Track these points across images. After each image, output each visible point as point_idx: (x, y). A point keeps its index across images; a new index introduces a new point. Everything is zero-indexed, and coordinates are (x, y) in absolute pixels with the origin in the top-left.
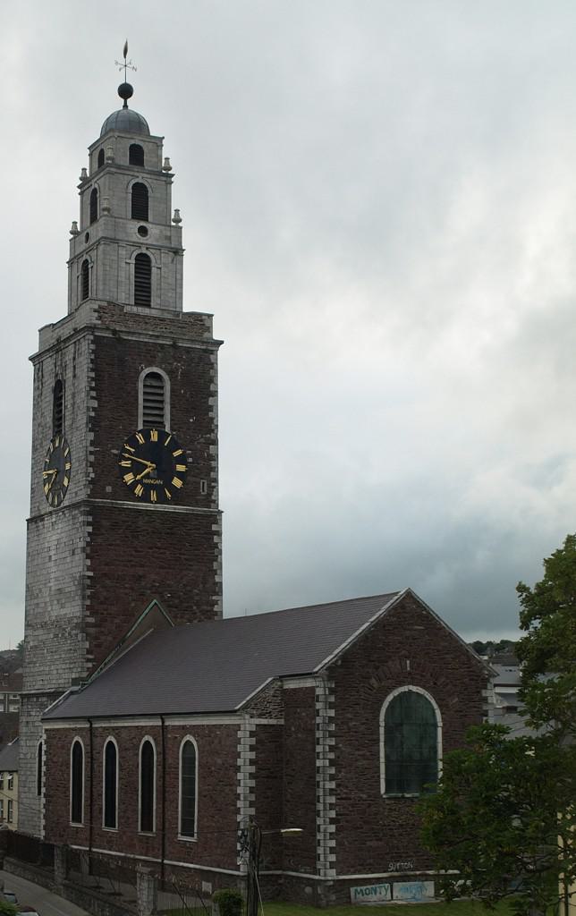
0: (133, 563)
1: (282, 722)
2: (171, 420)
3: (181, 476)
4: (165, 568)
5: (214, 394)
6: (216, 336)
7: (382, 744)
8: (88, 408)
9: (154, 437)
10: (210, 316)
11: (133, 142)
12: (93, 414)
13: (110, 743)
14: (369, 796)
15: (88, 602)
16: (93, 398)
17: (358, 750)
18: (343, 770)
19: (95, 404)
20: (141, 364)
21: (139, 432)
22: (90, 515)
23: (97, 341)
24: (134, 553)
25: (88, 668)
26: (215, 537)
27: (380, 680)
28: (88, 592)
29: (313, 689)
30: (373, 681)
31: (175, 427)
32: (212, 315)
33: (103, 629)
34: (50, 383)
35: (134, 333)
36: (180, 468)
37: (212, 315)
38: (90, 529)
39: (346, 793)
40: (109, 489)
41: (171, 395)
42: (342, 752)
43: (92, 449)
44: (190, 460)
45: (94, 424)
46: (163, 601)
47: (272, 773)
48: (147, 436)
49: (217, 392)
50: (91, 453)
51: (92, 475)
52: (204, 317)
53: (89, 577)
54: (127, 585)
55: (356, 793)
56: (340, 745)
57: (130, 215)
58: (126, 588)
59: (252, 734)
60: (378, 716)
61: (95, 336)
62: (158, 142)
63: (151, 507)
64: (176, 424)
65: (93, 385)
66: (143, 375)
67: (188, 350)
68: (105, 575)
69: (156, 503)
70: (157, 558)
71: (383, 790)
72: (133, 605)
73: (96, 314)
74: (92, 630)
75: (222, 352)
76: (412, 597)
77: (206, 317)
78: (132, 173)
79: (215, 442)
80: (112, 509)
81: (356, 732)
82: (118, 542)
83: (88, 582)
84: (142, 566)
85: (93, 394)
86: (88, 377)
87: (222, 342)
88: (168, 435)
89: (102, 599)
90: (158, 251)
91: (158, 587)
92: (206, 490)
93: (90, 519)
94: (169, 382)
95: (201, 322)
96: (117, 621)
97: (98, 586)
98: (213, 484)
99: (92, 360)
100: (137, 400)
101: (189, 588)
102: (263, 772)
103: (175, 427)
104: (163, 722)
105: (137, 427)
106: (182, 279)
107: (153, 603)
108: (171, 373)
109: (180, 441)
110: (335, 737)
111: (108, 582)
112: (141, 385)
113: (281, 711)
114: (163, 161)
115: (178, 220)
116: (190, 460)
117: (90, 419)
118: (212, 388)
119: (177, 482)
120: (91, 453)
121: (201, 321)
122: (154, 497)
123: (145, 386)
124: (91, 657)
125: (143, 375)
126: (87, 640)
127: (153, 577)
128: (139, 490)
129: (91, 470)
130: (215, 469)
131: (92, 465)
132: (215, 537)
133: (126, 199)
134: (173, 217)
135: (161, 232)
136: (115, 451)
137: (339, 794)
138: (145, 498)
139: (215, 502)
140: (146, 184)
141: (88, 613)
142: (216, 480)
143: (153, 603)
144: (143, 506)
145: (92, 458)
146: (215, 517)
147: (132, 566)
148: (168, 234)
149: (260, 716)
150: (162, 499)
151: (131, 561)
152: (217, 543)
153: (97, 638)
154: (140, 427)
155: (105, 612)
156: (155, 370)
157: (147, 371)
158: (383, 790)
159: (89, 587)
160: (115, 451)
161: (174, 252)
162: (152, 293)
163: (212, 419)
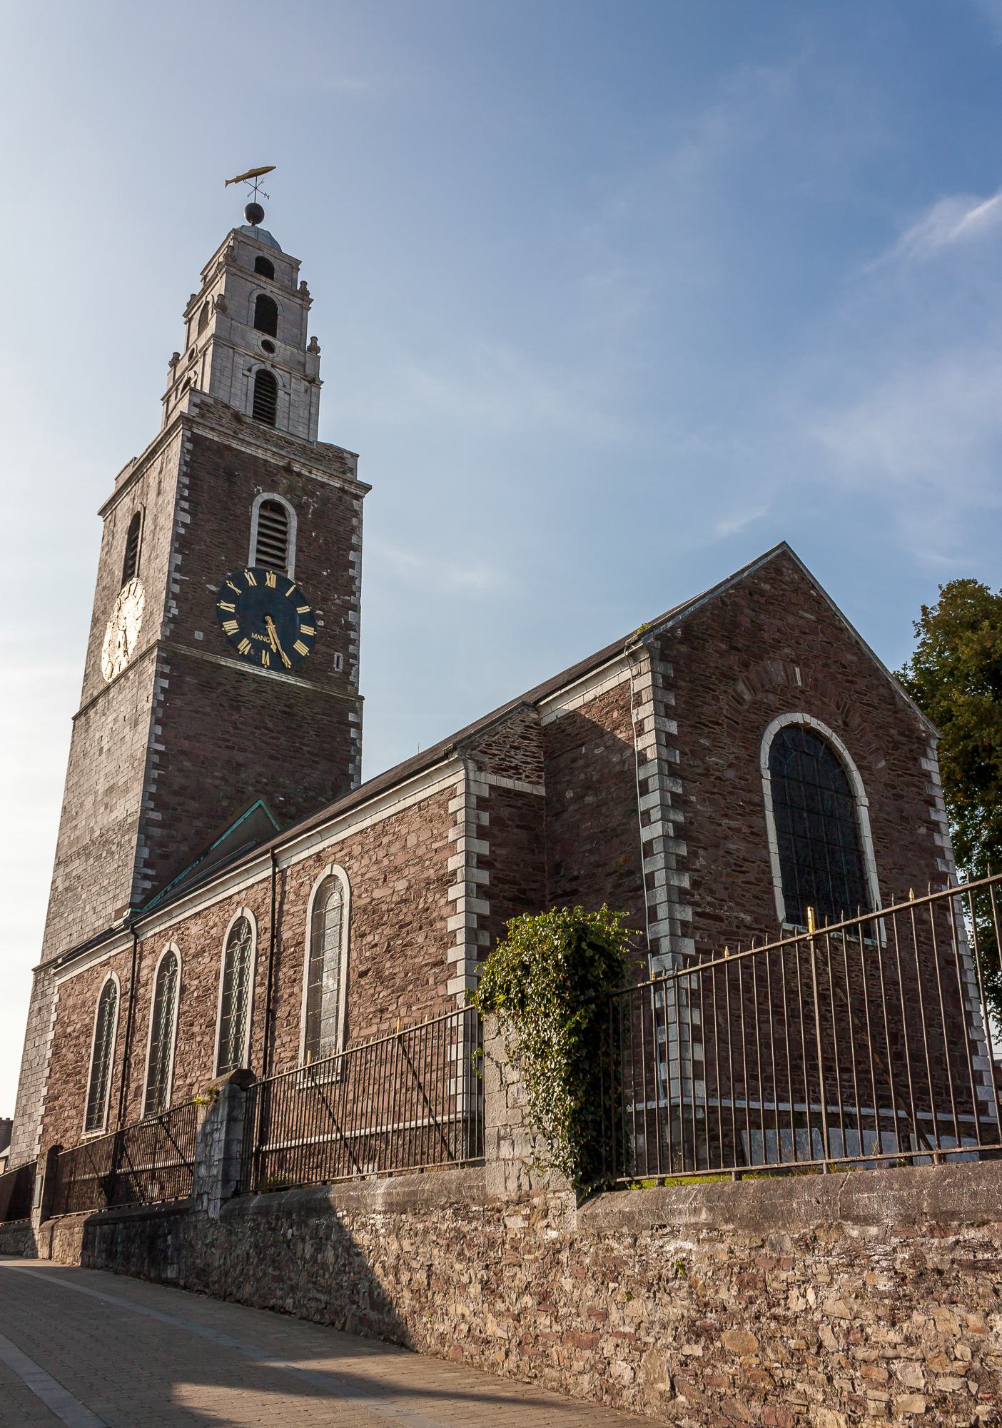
0: (230, 744)
1: (541, 791)
2: (297, 566)
3: (306, 639)
4: (277, 759)
5: (358, 548)
6: (361, 477)
7: (770, 815)
8: (176, 522)
9: (271, 581)
10: (356, 456)
11: (260, 254)
12: (182, 531)
13: (170, 954)
14: (756, 920)
15: (153, 789)
16: (183, 510)
17: (726, 815)
18: (701, 852)
19: (187, 519)
20: (256, 485)
21: (250, 570)
22: (168, 663)
23: (195, 439)
24: (231, 729)
25: (144, 889)
26: (353, 730)
27: (753, 689)
28: (155, 773)
29: (624, 686)
30: (741, 687)
31: (303, 576)
32: (358, 456)
33: (174, 833)
34: (124, 523)
35: (249, 444)
36: (307, 630)
37: (358, 456)
38: (166, 684)
39: (709, 904)
40: (199, 635)
41: (298, 534)
42: (697, 813)
43: (177, 576)
44: (321, 623)
45: (181, 543)
46: (273, 806)
47: (523, 892)
48: (260, 577)
49: (361, 546)
50: (175, 581)
51: (175, 611)
52: (345, 455)
53: (157, 752)
54: (216, 774)
55: (730, 907)
56: (693, 798)
57: (252, 323)
58: (214, 777)
59: (482, 804)
60: (758, 757)
61: (192, 432)
62: (294, 265)
63: (264, 673)
64: (303, 573)
65: (186, 493)
66: (259, 500)
67: (323, 485)
68: (184, 753)
69: (268, 668)
70: (266, 743)
71: (781, 915)
72: (225, 803)
73: (197, 410)
74: (156, 832)
75: (368, 500)
76: (790, 559)
77: (350, 456)
78: (257, 282)
79: (356, 608)
80: (199, 664)
81: (718, 778)
82: (208, 709)
83: (156, 759)
84: (244, 750)
85: (186, 505)
86: (179, 482)
87: (367, 488)
88: (291, 584)
89: (176, 787)
90: (287, 375)
91: (266, 784)
92: (341, 667)
93: (167, 670)
94: (296, 518)
95: (341, 461)
96: (198, 823)
97: (171, 768)
98: (351, 661)
99: (185, 461)
100: (249, 529)
101: (311, 794)
102: (506, 887)
103: (303, 576)
104: (275, 865)
105: (247, 563)
106: (317, 414)
107: (257, 805)
108: (300, 508)
109: (306, 595)
110: (682, 778)
111: (187, 764)
112: (255, 512)
113: (541, 769)
114: (299, 286)
115: (314, 349)
116: (321, 623)
117: (176, 537)
118: (354, 540)
119: (301, 648)
120: (175, 581)
121: (342, 458)
122: (266, 659)
123: (261, 516)
124: (150, 872)
125: (259, 500)
126: (146, 845)
127: (258, 768)
128: (244, 646)
129: (173, 603)
130: (355, 642)
131: (175, 597)
132: (353, 730)
133: (248, 308)
134: (308, 343)
135: (292, 354)
136: (213, 588)
137: (698, 905)
138: (254, 659)
139: (355, 685)
140: (275, 299)
141: (152, 804)
142: (356, 657)
143: (257, 805)
144: (248, 668)
145: (176, 589)
146: (356, 703)
147: (228, 747)
148: (302, 359)
149: (498, 770)
150: (277, 664)
151: (229, 741)
152: (355, 739)
153: (162, 845)
154: (252, 564)
155: (180, 808)
156: (277, 497)
157: (266, 496)
158: (781, 915)
159: (156, 766)
160: (213, 588)
161: (310, 382)
162: (277, 420)
163: (352, 579)
